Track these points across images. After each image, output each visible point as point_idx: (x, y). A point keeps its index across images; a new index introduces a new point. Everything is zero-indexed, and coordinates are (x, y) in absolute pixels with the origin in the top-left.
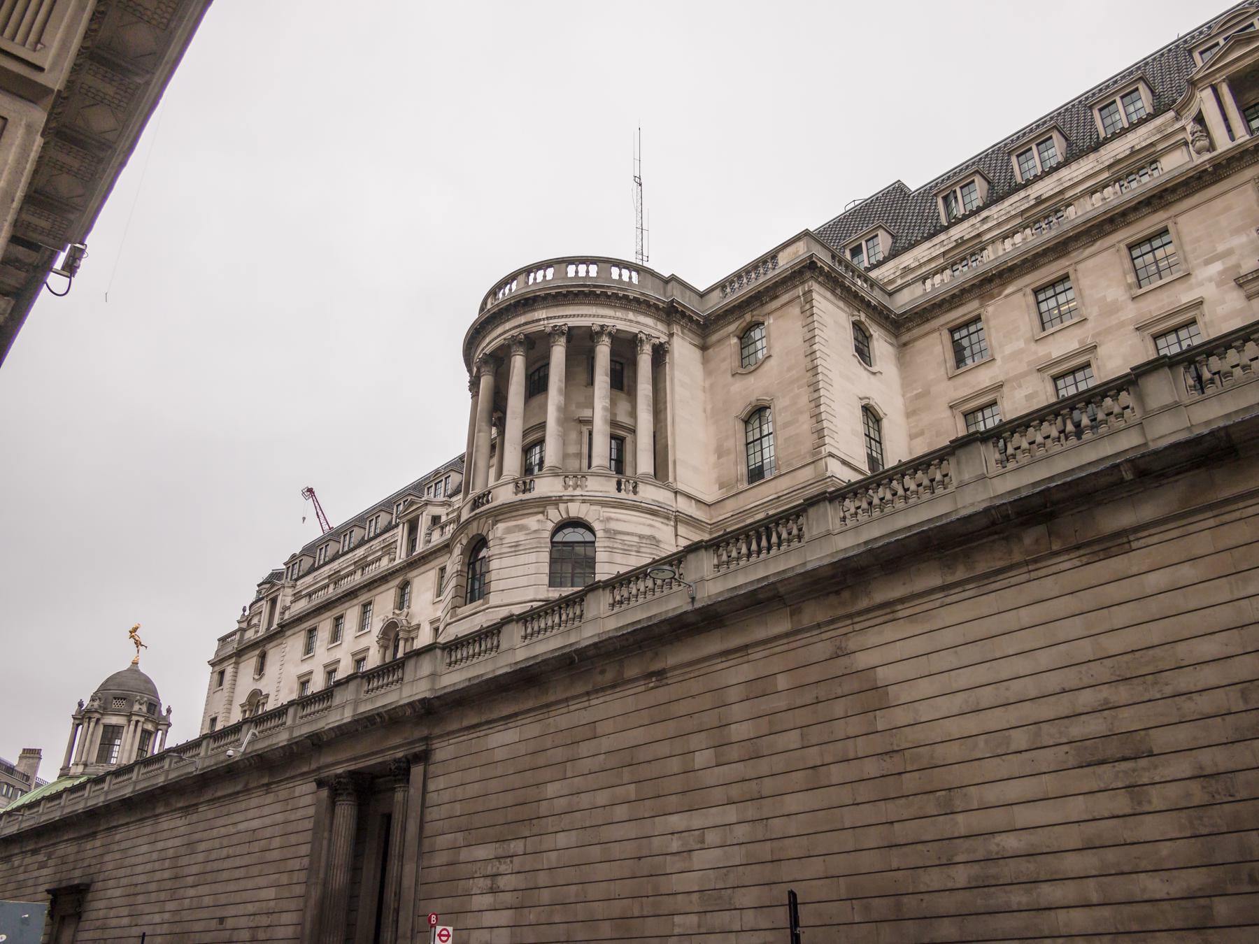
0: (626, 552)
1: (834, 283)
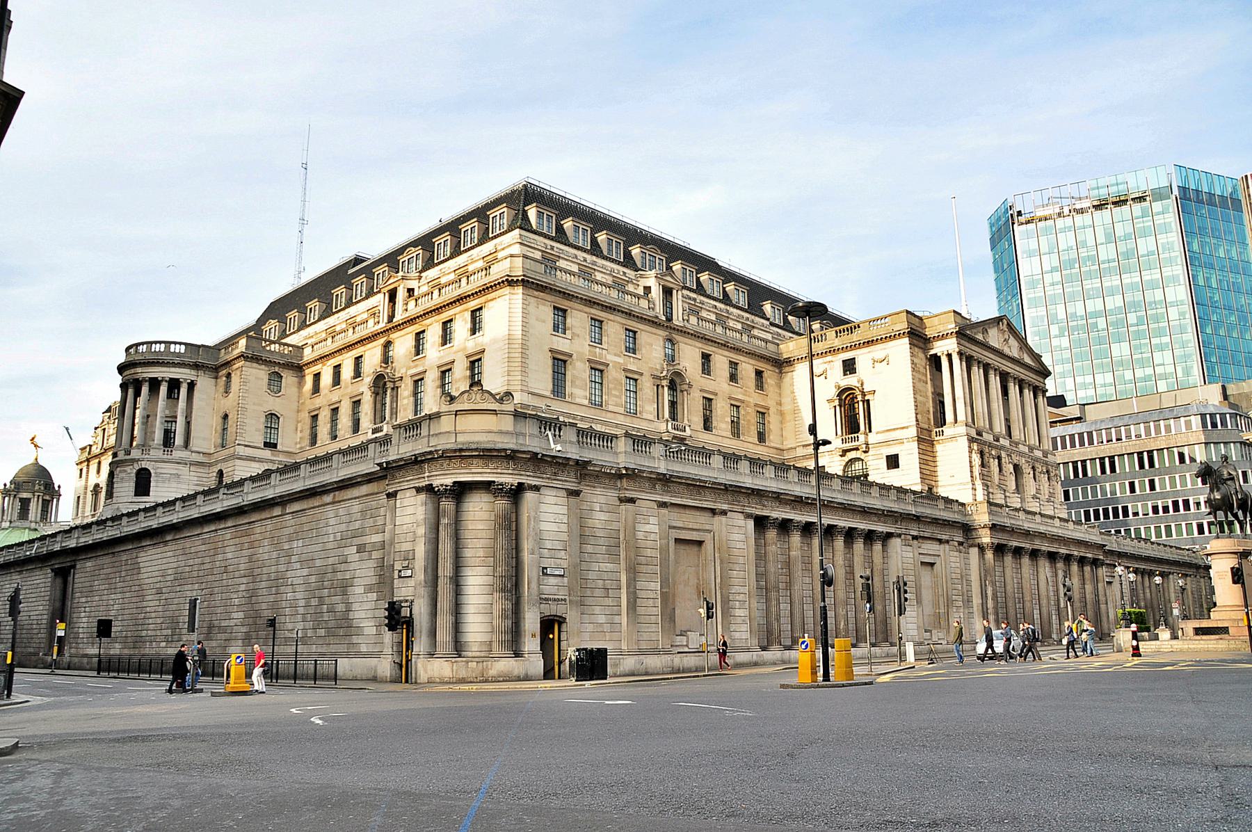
0: (164, 482)
1: (255, 359)
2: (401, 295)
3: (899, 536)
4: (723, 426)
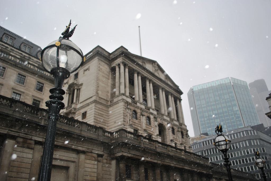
3: (13, 138)
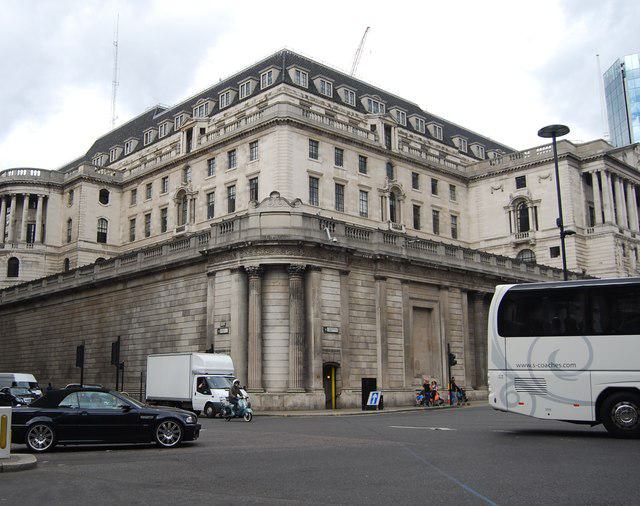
1: (91, 180)
2: (196, 133)
4: (427, 226)
